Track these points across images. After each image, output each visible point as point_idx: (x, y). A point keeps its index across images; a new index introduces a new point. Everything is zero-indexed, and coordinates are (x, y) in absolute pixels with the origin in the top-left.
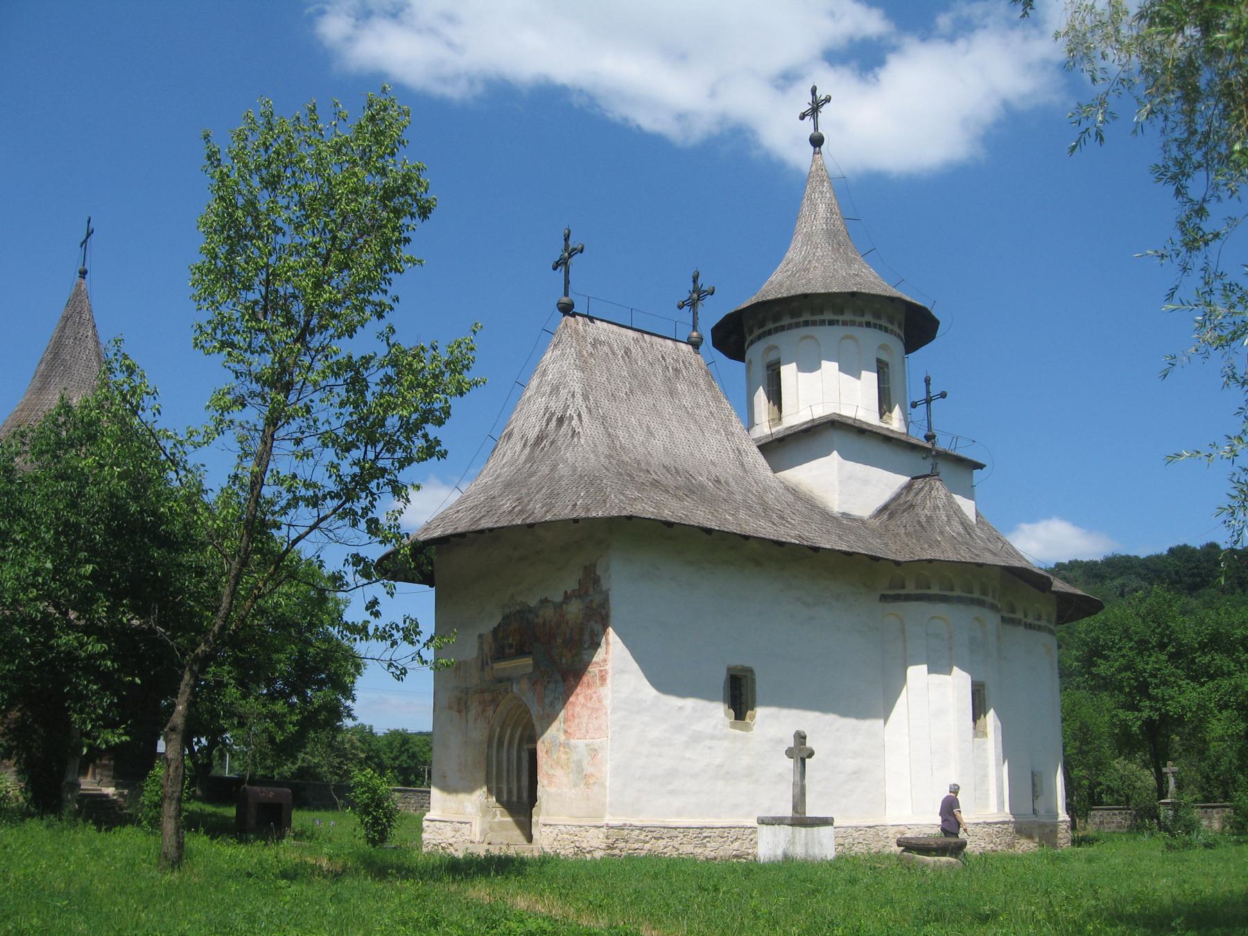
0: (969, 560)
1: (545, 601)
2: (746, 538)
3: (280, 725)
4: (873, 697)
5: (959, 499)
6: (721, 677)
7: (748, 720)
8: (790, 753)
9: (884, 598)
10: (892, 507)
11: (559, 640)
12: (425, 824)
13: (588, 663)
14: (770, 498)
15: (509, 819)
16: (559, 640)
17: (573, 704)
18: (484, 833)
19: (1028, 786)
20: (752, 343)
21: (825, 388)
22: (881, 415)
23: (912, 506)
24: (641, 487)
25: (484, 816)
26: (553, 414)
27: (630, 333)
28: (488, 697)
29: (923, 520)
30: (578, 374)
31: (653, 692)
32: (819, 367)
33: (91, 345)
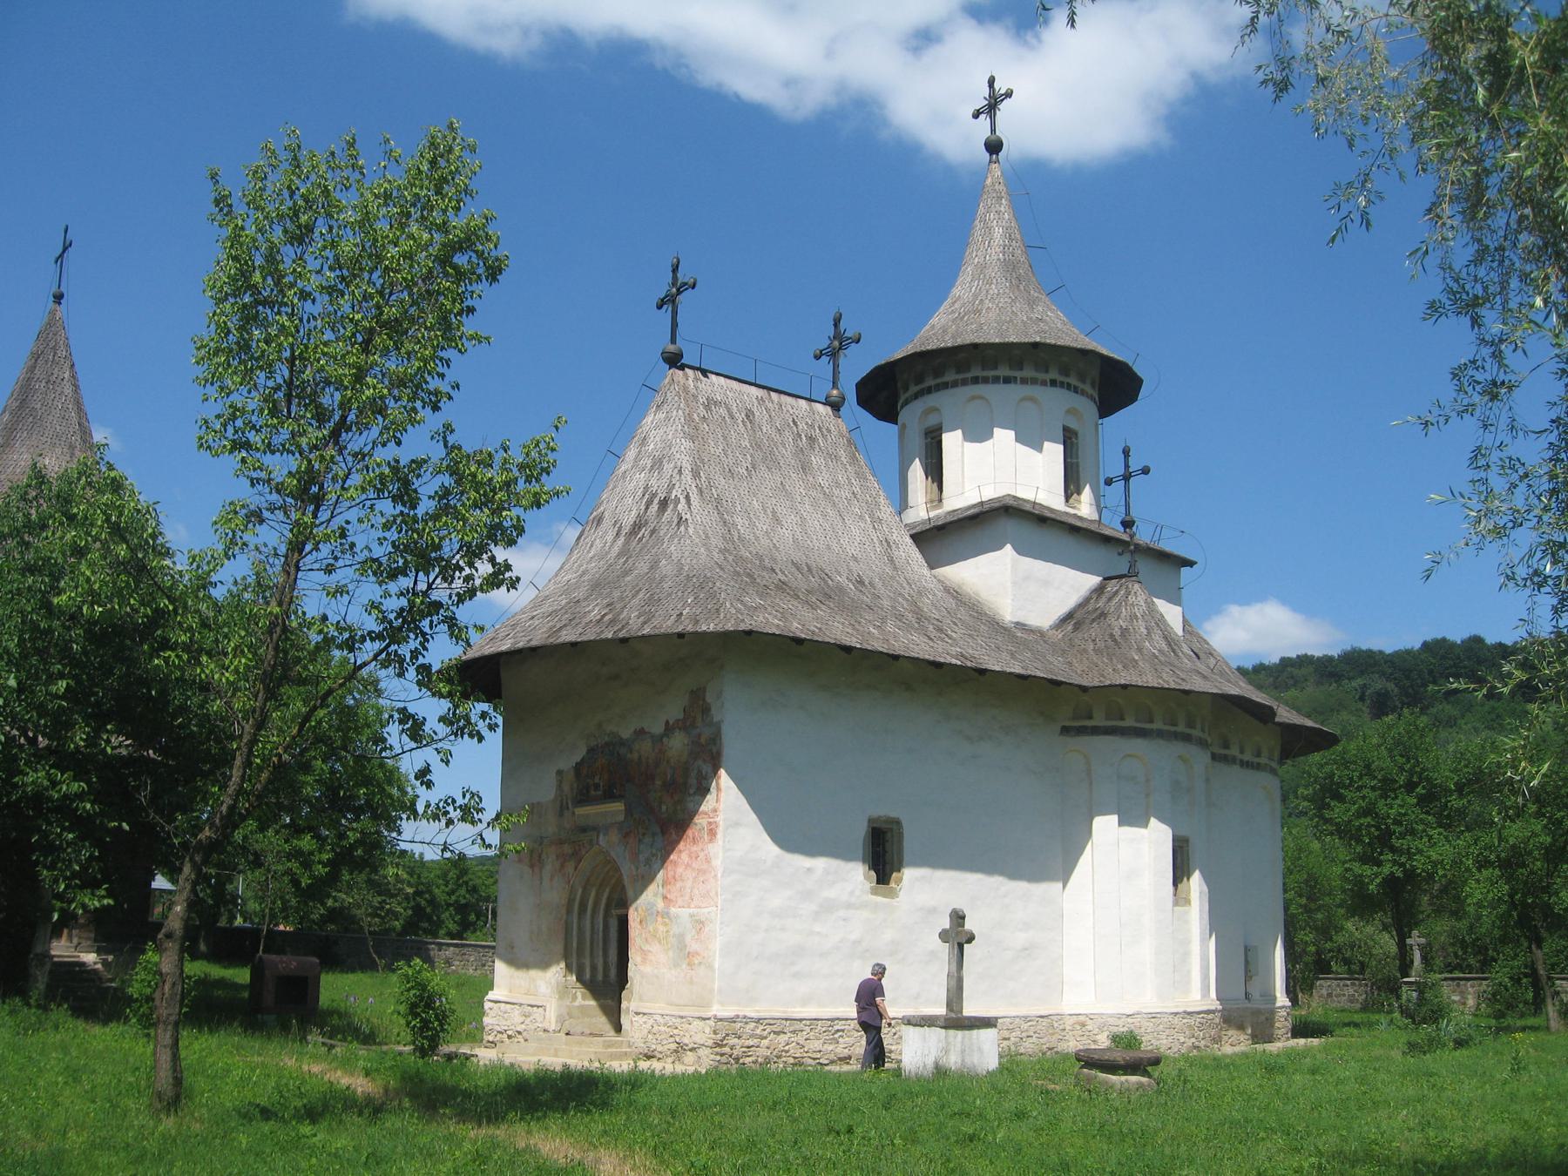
0: (1173, 686)
1: (641, 733)
2: (896, 657)
3: (307, 865)
4: (1050, 855)
5: (1162, 606)
6: (861, 831)
7: (892, 884)
8: (944, 936)
9: (1065, 730)
10: (1078, 615)
11: (658, 783)
12: (487, 1005)
13: (692, 814)
14: (926, 604)
15: (593, 1003)
16: (658, 783)
17: (675, 863)
18: (561, 1020)
19: (1239, 963)
20: (906, 403)
21: (997, 462)
22: (1068, 497)
23: (1103, 615)
24: (764, 591)
25: (561, 998)
26: (654, 495)
27: (754, 391)
28: (567, 849)
29: (1117, 632)
30: (687, 444)
31: (774, 850)
32: (990, 435)
33: (68, 390)
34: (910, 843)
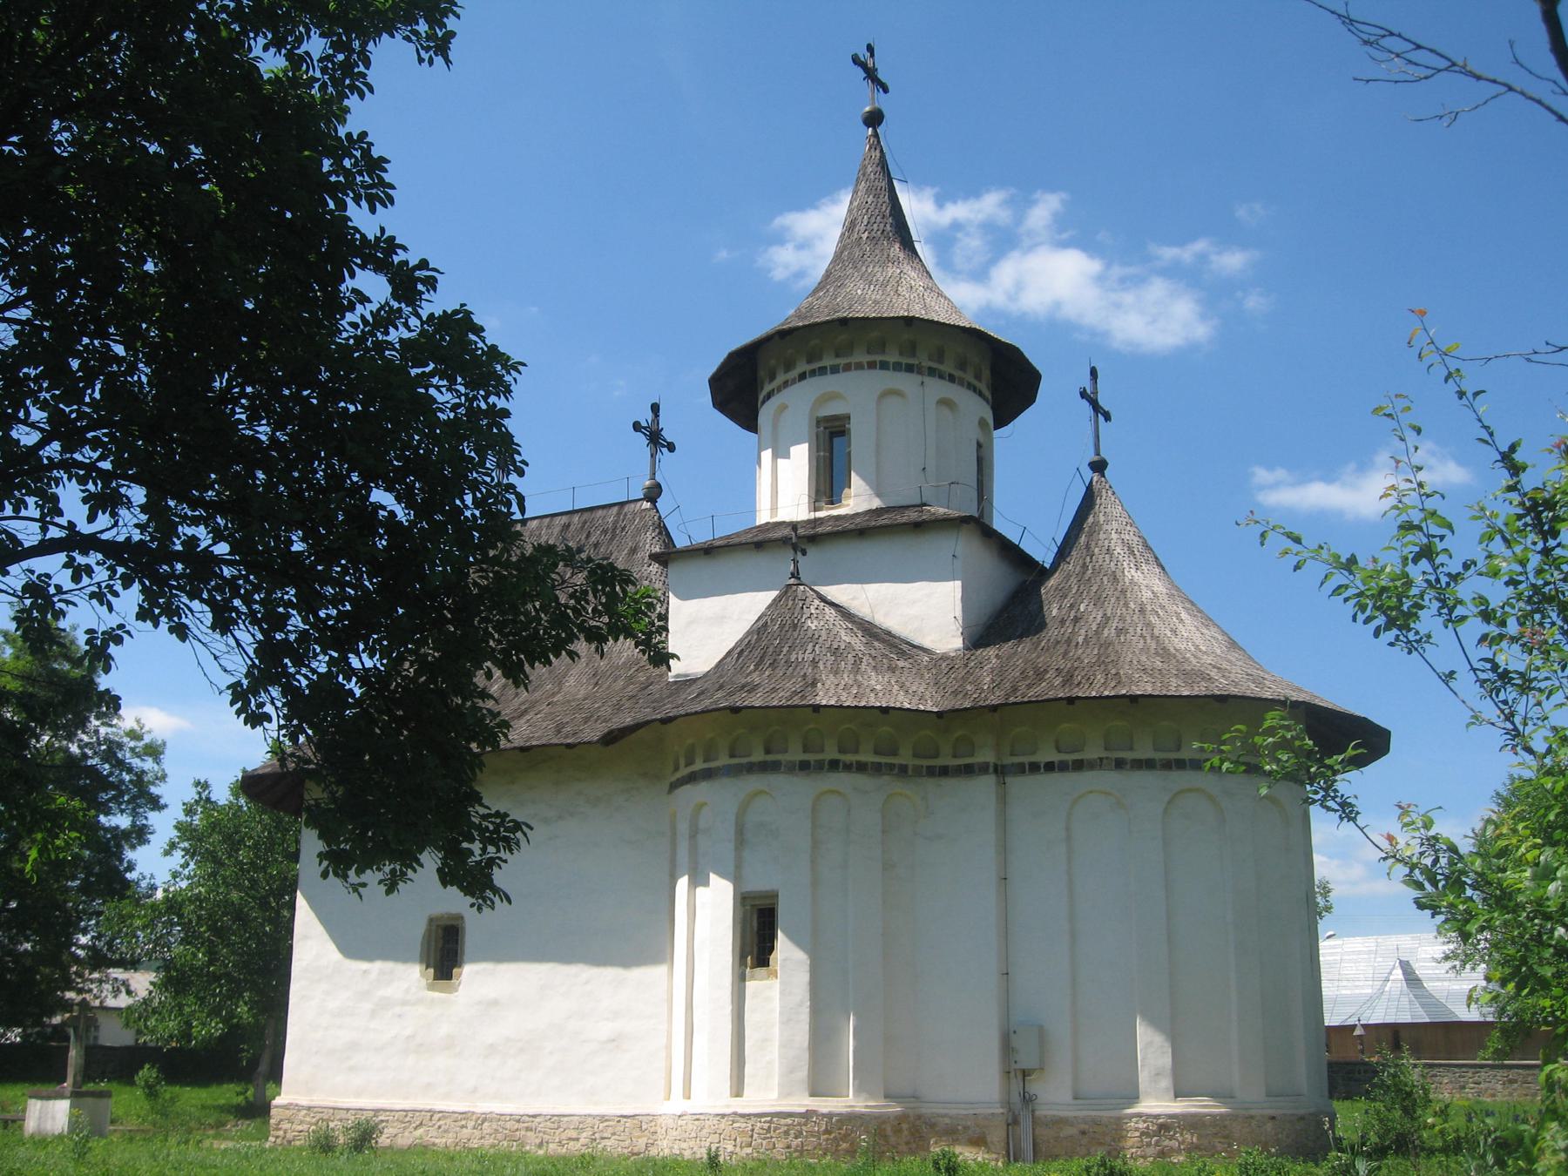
34: (471, 938)
